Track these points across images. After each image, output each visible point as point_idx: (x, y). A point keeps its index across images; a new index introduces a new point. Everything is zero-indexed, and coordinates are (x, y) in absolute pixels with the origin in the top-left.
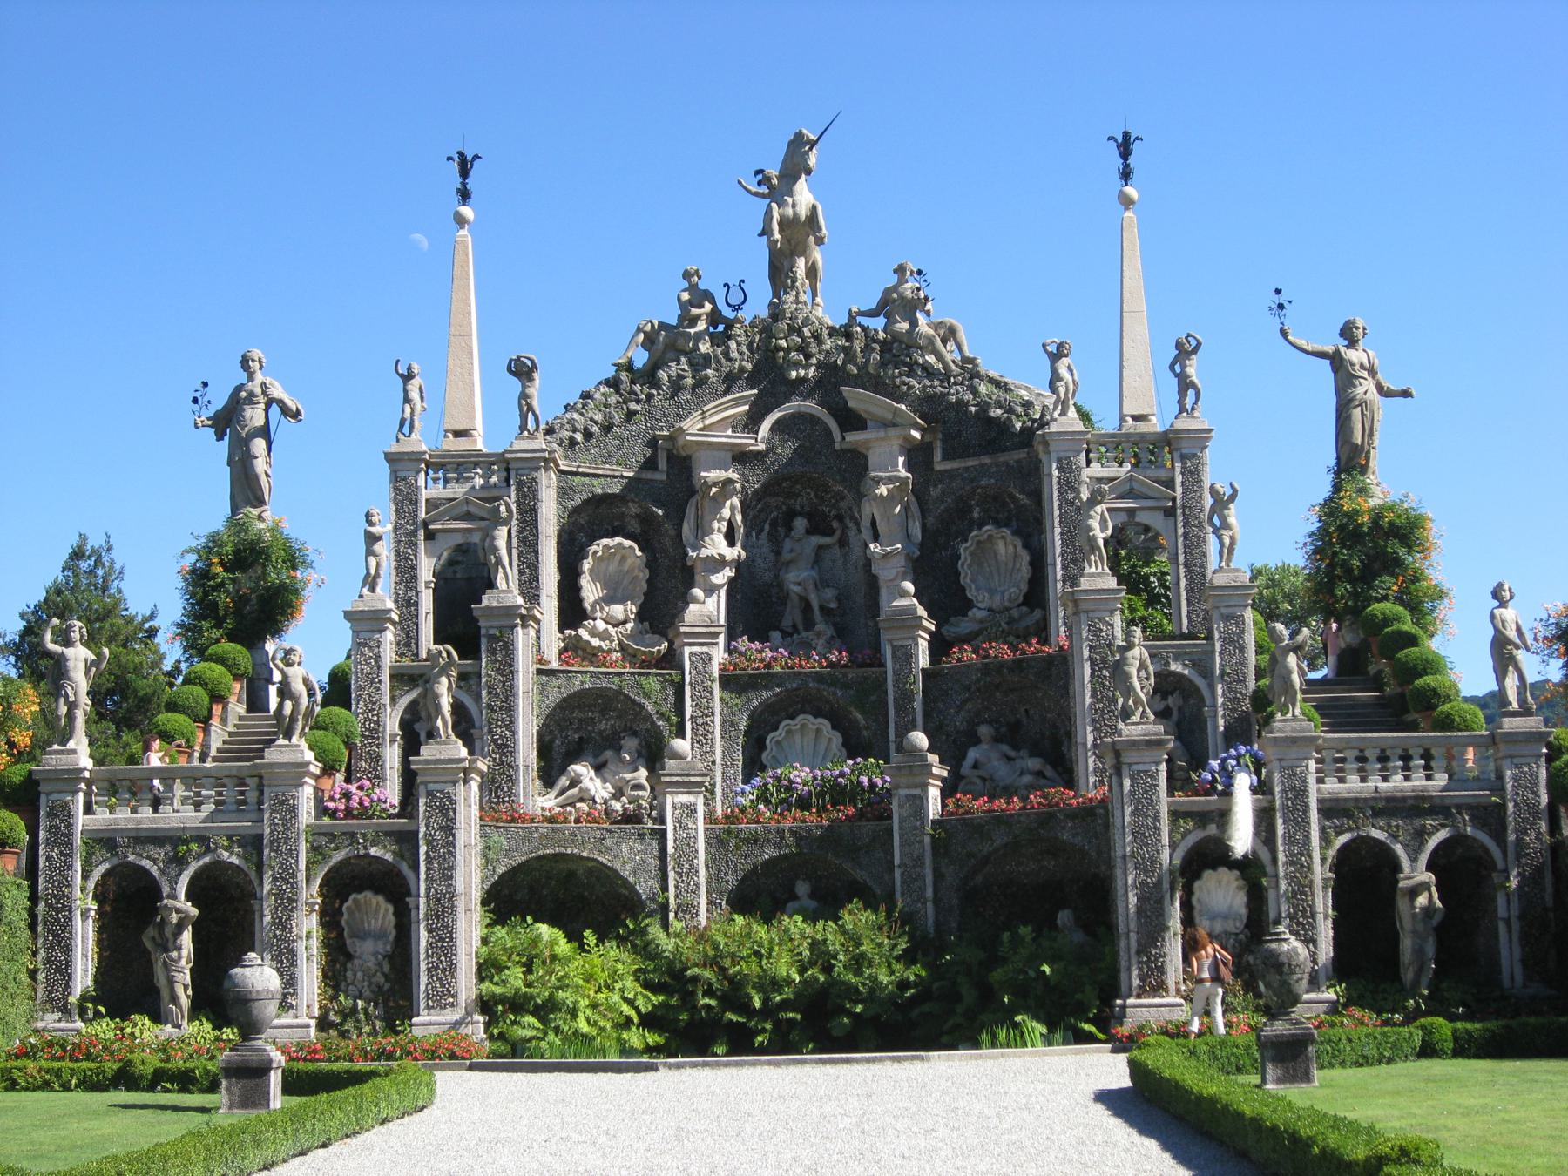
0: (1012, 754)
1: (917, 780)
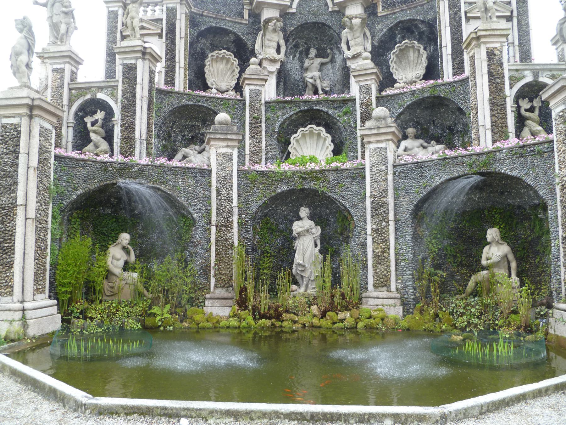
0: (425, 144)
1: (383, 138)
